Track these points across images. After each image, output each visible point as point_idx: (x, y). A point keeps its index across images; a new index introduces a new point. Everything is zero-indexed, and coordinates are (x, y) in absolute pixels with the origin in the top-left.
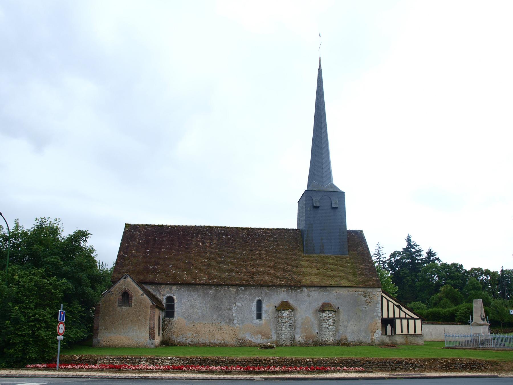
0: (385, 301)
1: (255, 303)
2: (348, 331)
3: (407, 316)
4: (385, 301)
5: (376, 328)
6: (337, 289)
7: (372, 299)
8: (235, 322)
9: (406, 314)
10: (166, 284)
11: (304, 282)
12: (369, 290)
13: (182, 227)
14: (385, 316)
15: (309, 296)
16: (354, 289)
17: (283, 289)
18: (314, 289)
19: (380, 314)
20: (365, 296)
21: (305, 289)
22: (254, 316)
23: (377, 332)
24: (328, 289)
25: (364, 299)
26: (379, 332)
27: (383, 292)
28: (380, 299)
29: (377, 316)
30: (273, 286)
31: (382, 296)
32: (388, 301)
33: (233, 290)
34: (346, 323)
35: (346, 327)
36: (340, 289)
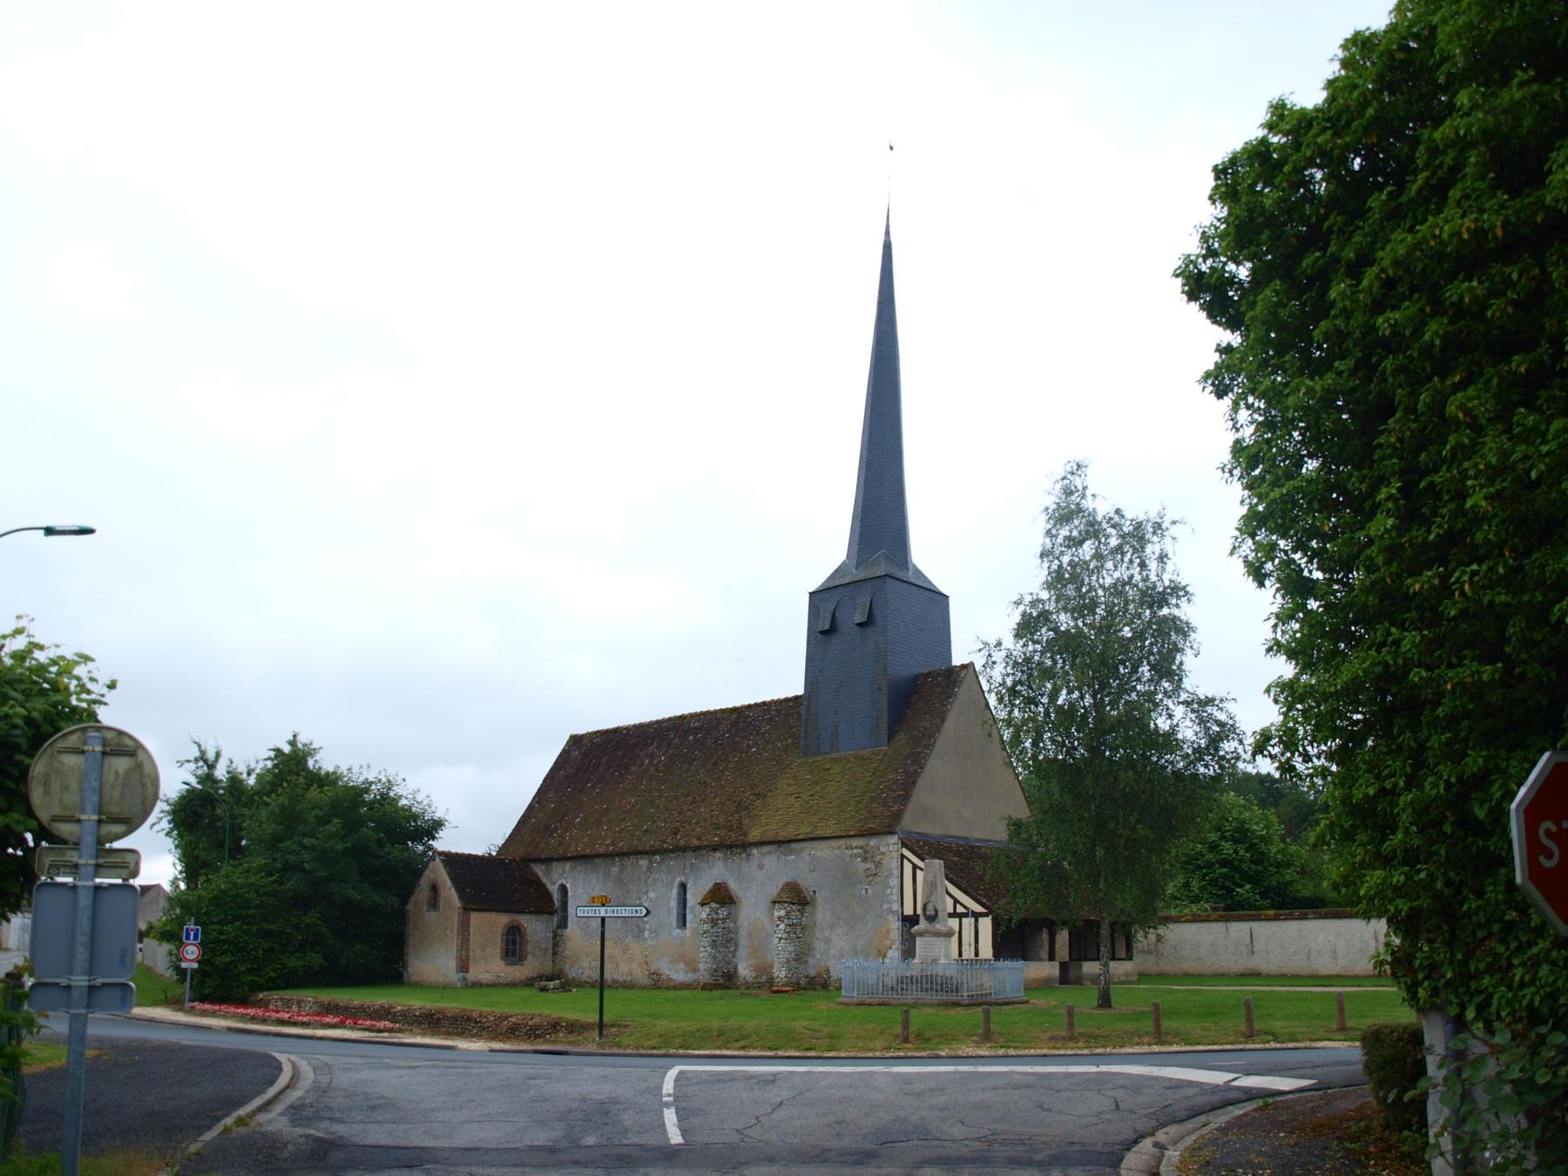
0: (908, 867)
1: (675, 891)
2: (833, 952)
3: (960, 909)
4: (908, 867)
5: (888, 942)
6: (809, 844)
7: (878, 865)
8: (646, 934)
9: (956, 901)
10: (558, 860)
11: (751, 838)
12: (873, 842)
13: (663, 721)
14: (909, 911)
15: (761, 867)
16: (841, 842)
17: (718, 854)
18: (767, 848)
19: (896, 907)
20: (865, 860)
21: (755, 851)
22: (674, 919)
23: (890, 953)
24: (794, 846)
25: (862, 866)
26: (894, 954)
27: (904, 845)
28: (895, 864)
29: (890, 911)
30: (701, 849)
31: (903, 856)
32: (915, 867)
33: (643, 862)
34: (827, 933)
35: (828, 941)
36: (815, 844)
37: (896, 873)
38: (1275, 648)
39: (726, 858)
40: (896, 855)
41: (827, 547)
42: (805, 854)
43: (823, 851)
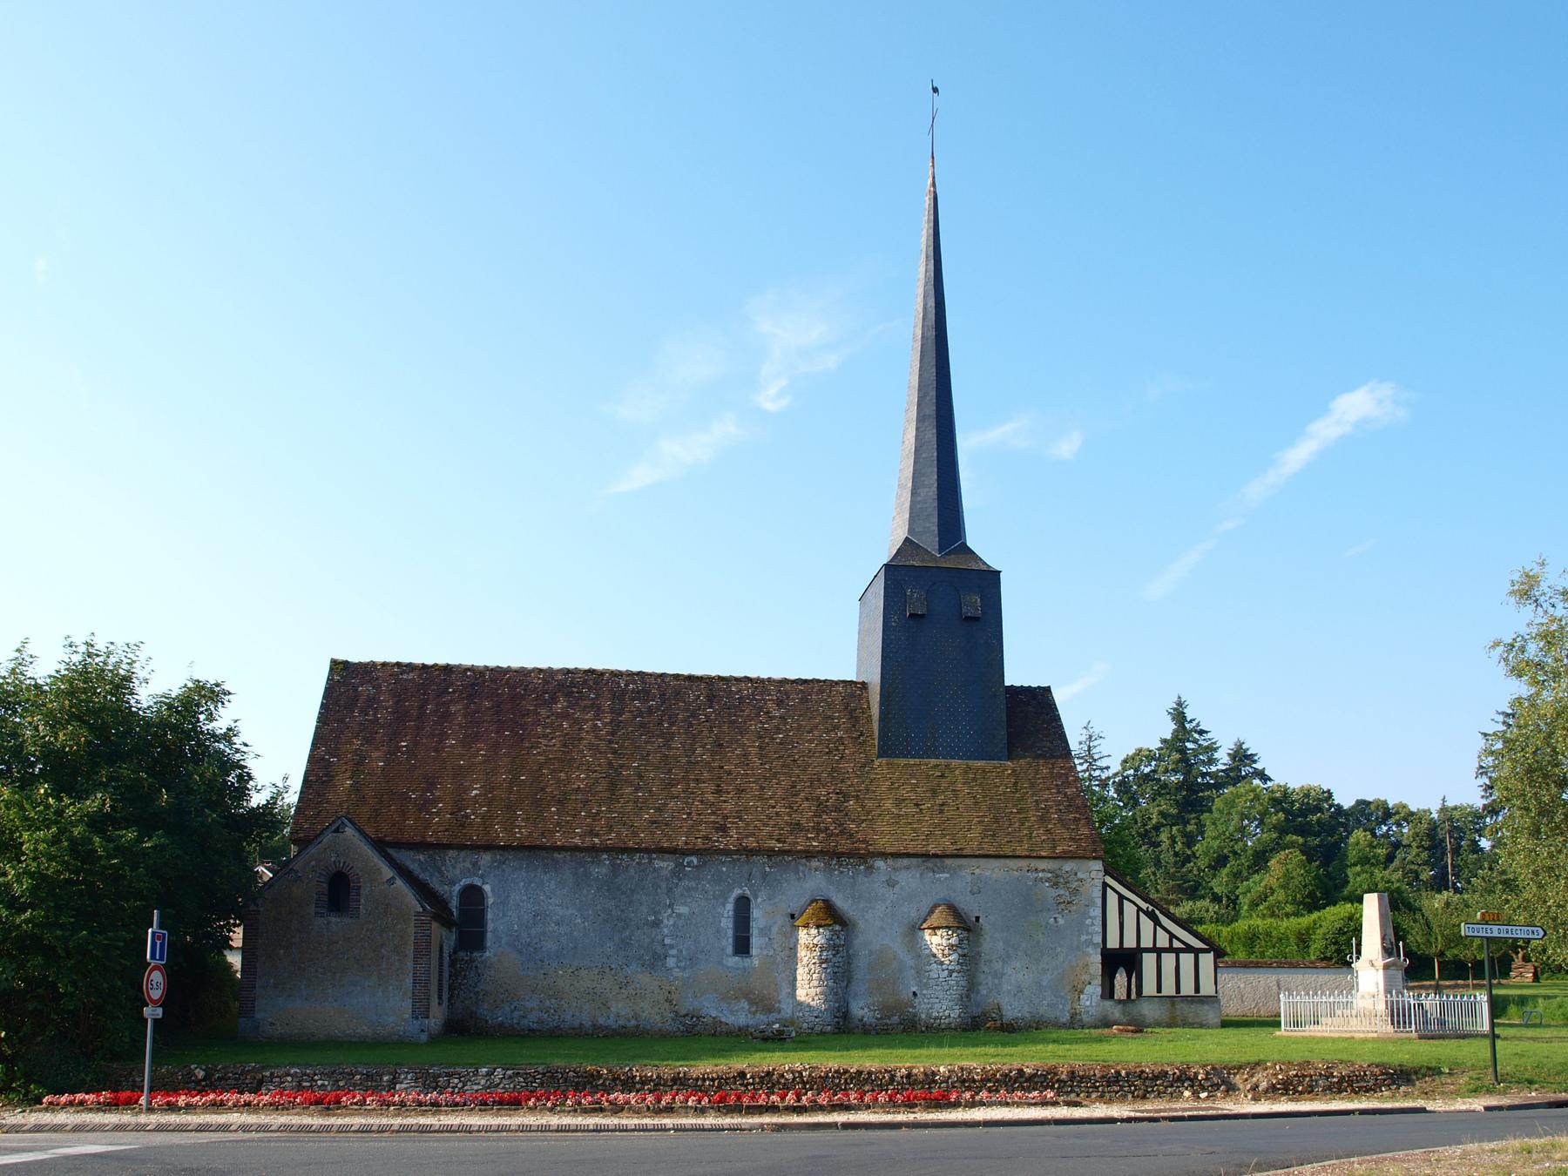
0: (1112, 899)
1: (730, 907)
2: (1006, 987)
3: (1176, 944)
4: (1112, 899)
5: (1086, 977)
6: (973, 861)
7: (1075, 892)
8: (671, 962)
9: (1172, 936)
10: (461, 847)
11: (883, 842)
12: (1068, 866)
13: (508, 670)
14: (1113, 943)
15: (891, 884)
16: (1024, 863)
17: (815, 863)
18: (906, 861)
19: (1098, 939)
20: (1056, 885)
21: (880, 863)
22: (728, 944)
23: (1088, 989)
24: (948, 861)
25: (1053, 892)
26: (1095, 989)
27: (1107, 873)
28: (1098, 893)
29: (1090, 943)
30: (785, 856)
31: (1105, 885)
32: (1121, 898)
33: (665, 865)
34: (998, 966)
35: (999, 975)
36: (982, 861)
37: (1099, 902)
38: (229, 735)
39: (828, 869)
40: (1099, 883)
41: (882, 526)
42: (965, 873)
43: (993, 870)
